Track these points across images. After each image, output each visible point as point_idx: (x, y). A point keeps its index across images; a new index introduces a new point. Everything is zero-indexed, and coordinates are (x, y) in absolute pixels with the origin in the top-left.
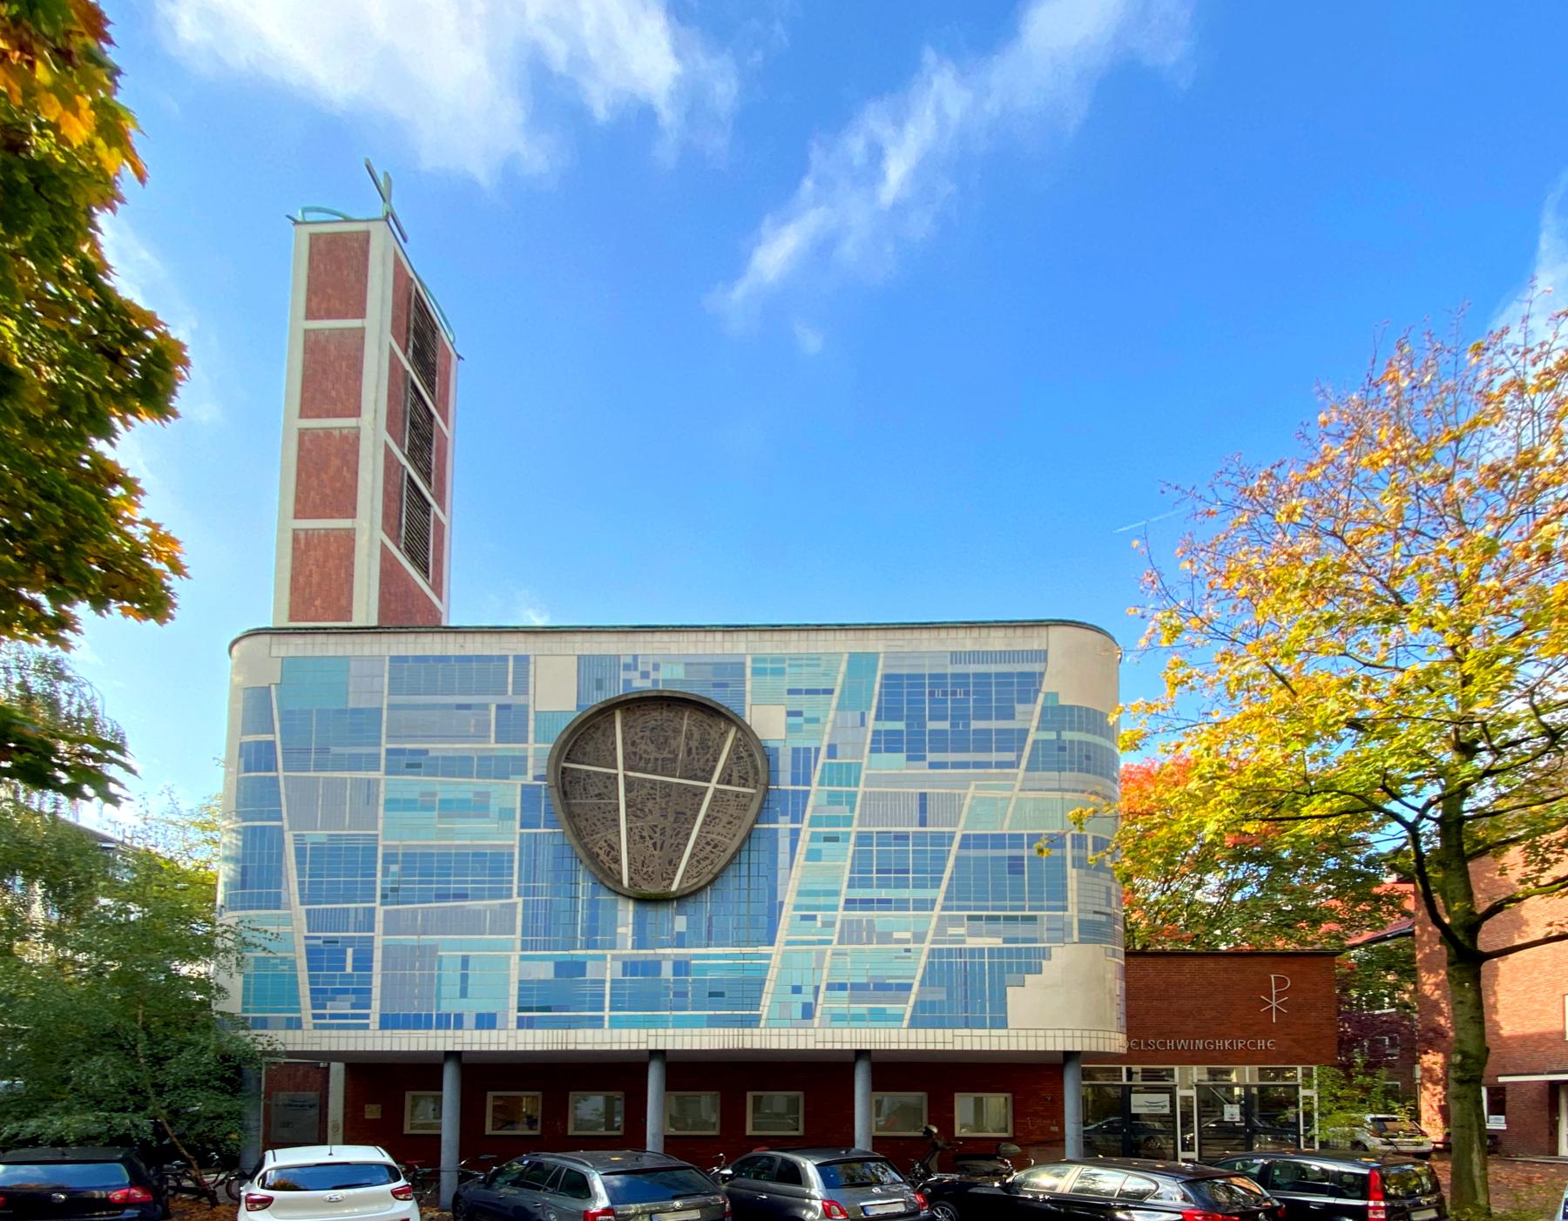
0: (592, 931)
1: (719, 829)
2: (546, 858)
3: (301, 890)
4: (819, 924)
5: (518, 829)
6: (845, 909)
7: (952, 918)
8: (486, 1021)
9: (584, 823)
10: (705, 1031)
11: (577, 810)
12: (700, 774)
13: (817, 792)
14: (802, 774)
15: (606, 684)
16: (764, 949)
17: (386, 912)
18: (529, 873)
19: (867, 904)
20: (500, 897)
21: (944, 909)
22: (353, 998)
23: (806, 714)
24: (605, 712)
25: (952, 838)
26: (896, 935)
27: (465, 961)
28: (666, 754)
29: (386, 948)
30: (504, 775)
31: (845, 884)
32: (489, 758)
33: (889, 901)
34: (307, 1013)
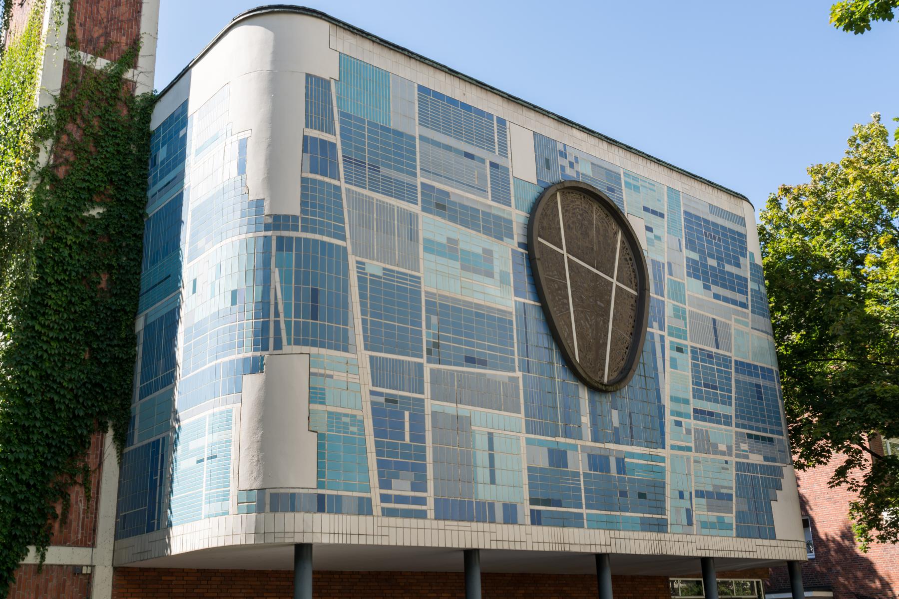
3: (365, 330)
8: (511, 516)
10: (642, 535)
16: (660, 452)
17: (432, 370)
22: (412, 475)
27: (491, 436)
29: (434, 414)
33: (711, 414)
34: (375, 494)
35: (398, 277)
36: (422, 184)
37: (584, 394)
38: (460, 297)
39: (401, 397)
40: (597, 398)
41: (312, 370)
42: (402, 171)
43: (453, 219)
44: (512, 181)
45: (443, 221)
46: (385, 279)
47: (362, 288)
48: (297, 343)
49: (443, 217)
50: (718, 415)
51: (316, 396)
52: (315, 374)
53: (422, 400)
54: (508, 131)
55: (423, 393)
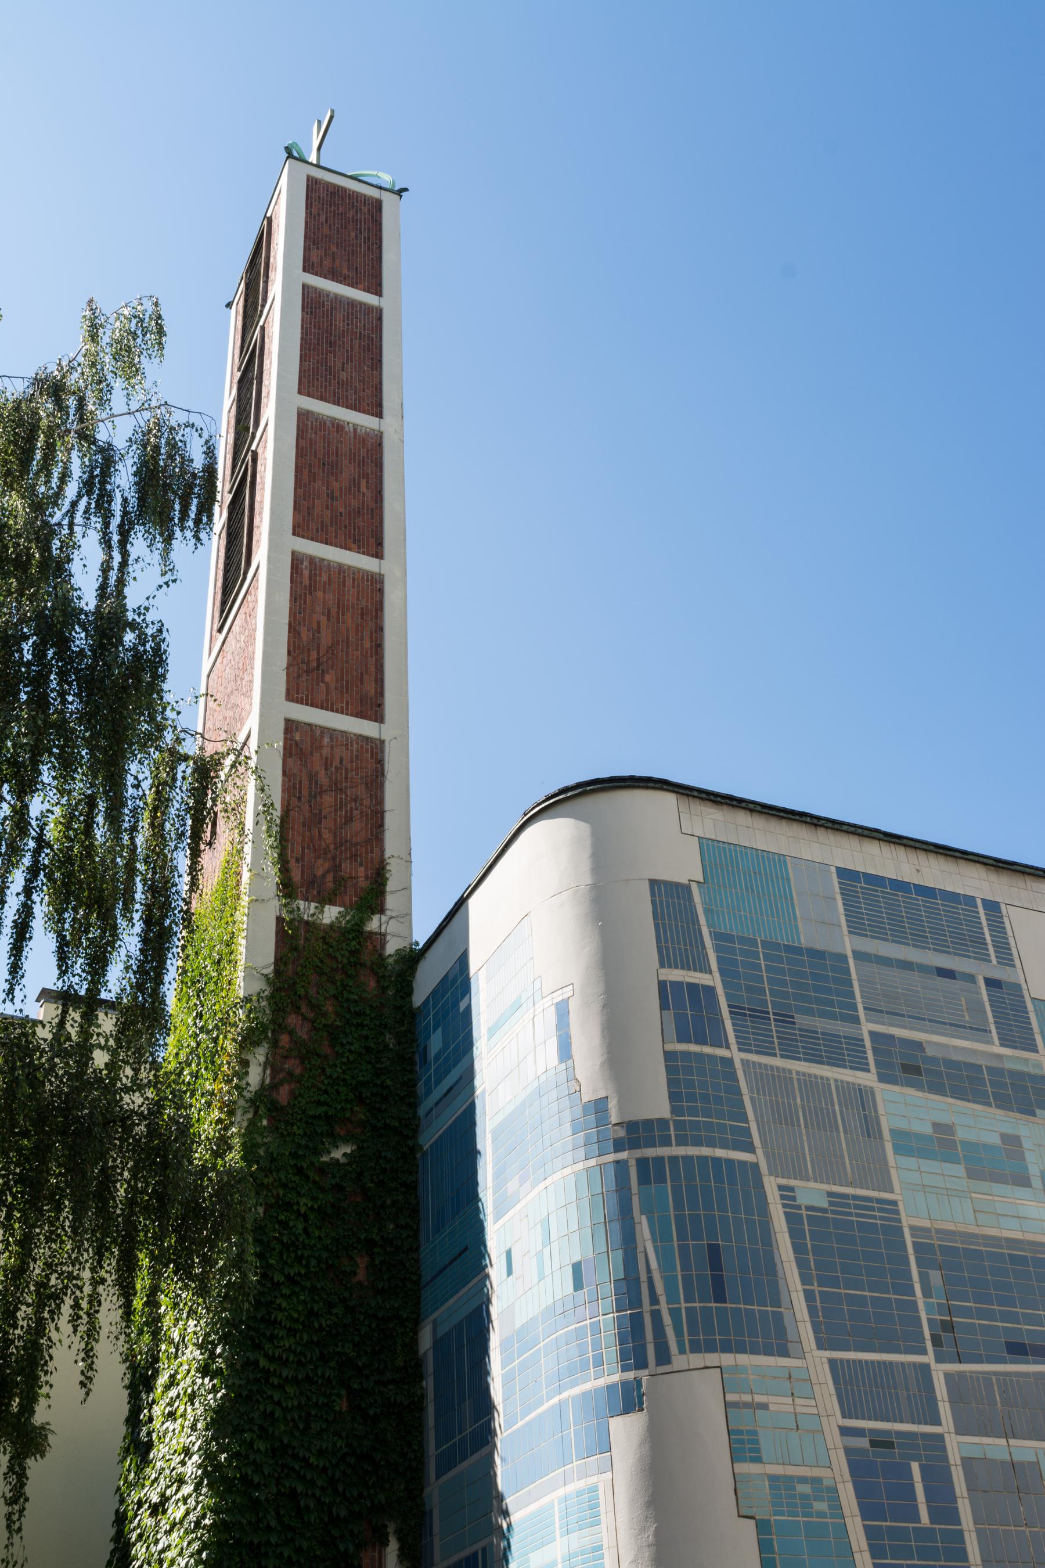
3: (812, 1311)
17: (948, 1376)
35: (856, 1207)
36: (871, 1033)
38: (976, 1230)
39: (899, 1434)
41: (730, 1397)
42: (832, 1016)
43: (937, 1089)
44: (1030, 1007)
45: (920, 1094)
46: (833, 1212)
47: (795, 1233)
48: (696, 1348)
49: (919, 1087)
51: (743, 1446)
52: (736, 1405)
53: (940, 1438)
54: (1006, 920)
55: (938, 1423)
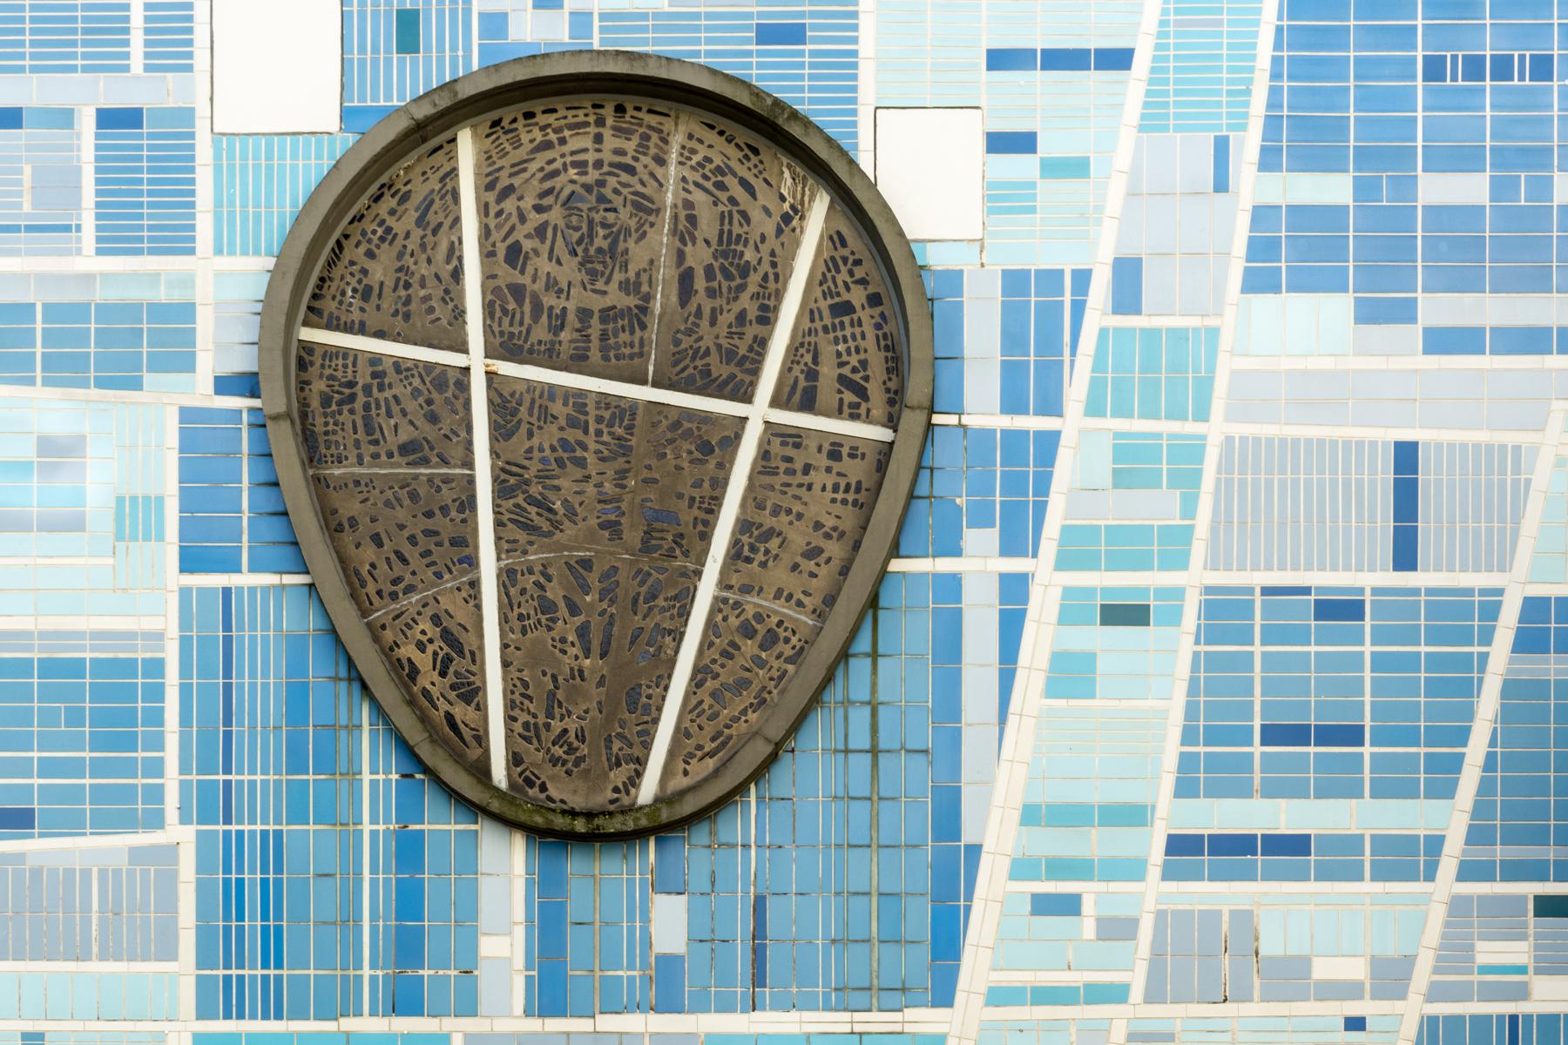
0: (406, 947)
1: (779, 575)
2: (262, 684)
4: (1088, 927)
5: (176, 579)
6: (1168, 874)
7: (1491, 906)
9: (369, 553)
11: (349, 506)
12: (721, 370)
13: (1083, 442)
14: (1032, 383)
15: (429, 31)
18: (216, 745)
19: (1232, 850)
20: (128, 822)
21: (1468, 872)
23: (1047, 146)
24: (427, 131)
25: (1491, 611)
26: (1322, 970)
28: (615, 297)
30: (122, 376)
31: (1168, 782)
32: (79, 311)
33: (1296, 845)
37: (506, 864)
40: (576, 865)
50: (1351, 843)
